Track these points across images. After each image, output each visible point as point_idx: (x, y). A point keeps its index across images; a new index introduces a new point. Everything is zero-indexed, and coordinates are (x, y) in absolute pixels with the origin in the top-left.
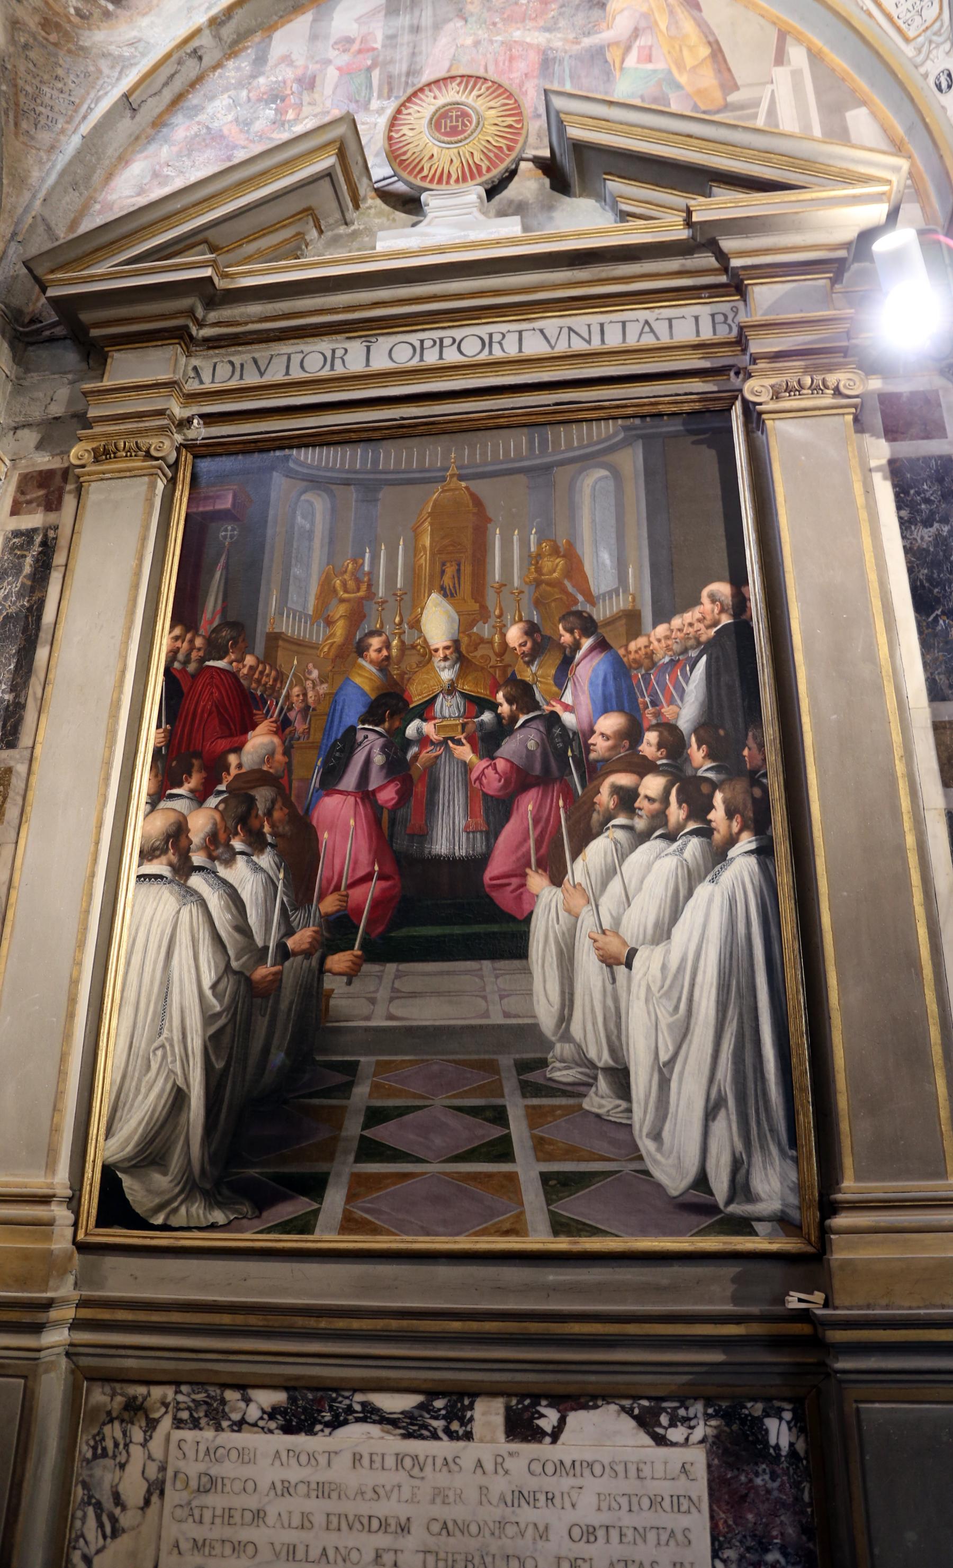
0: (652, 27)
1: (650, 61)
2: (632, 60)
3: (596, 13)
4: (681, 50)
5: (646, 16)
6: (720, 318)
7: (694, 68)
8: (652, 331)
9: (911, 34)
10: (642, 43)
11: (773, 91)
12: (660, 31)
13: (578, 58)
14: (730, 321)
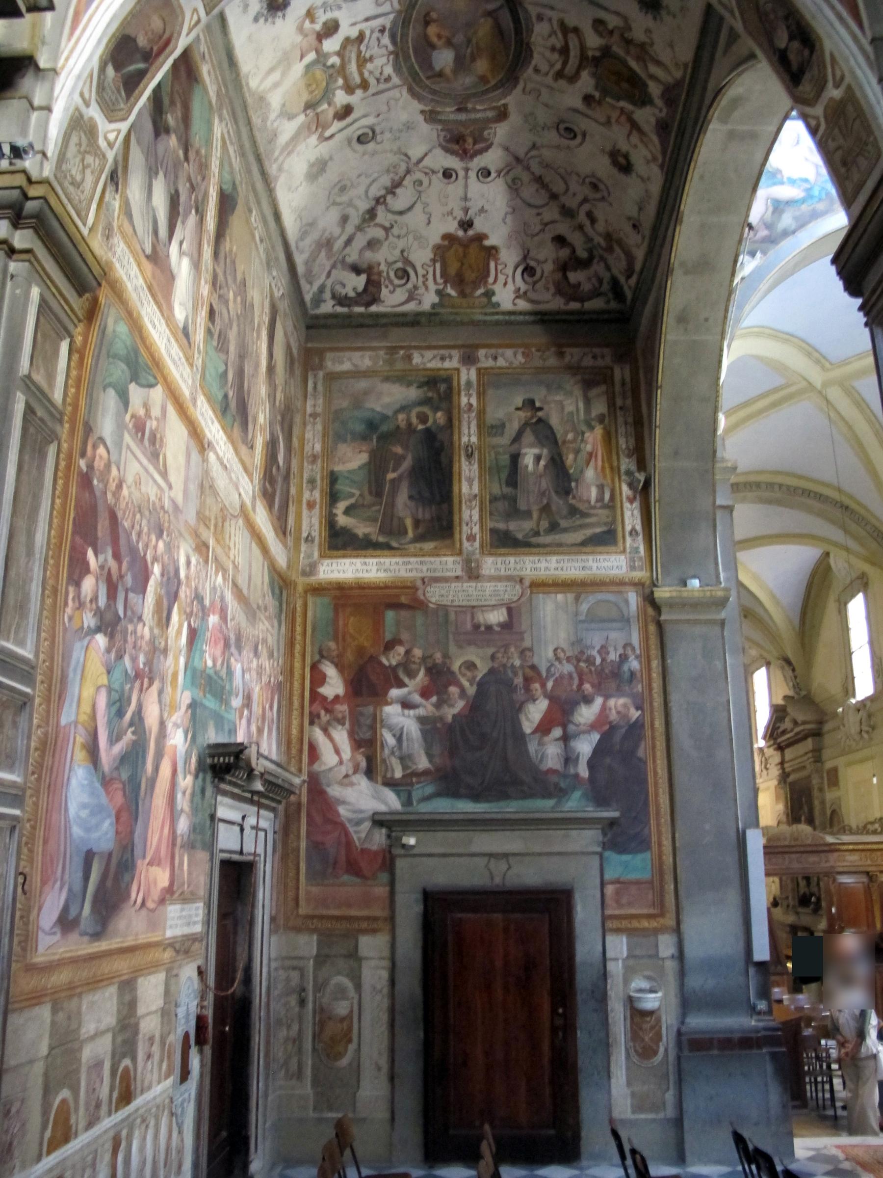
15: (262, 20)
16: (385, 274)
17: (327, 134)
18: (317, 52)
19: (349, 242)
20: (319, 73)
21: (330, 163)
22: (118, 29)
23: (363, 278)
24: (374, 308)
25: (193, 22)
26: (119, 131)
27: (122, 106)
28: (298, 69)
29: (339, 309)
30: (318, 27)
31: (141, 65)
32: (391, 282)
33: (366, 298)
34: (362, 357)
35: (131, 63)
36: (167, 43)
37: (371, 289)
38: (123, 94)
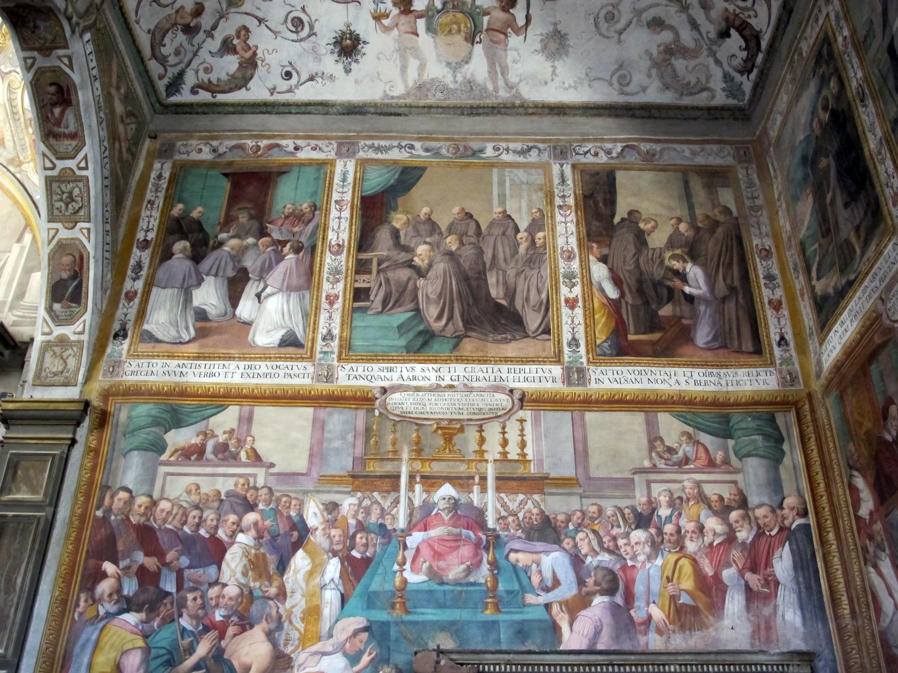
15: (354, 66)
16: (738, 11)
17: (521, 22)
18: (420, 17)
19: (695, 26)
20: (446, 19)
21: (559, 28)
22: (47, 288)
23: (733, 32)
24: (764, 44)
26: (85, 321)
27: (77, 310)
28: (425, 40)
29: (753, 76)
30: (395, 11)
32: (747, 9)
33: (753, 44)
34: (782, 98)
36: (82, 258)
37: (747, 33)
38: (74, 305)
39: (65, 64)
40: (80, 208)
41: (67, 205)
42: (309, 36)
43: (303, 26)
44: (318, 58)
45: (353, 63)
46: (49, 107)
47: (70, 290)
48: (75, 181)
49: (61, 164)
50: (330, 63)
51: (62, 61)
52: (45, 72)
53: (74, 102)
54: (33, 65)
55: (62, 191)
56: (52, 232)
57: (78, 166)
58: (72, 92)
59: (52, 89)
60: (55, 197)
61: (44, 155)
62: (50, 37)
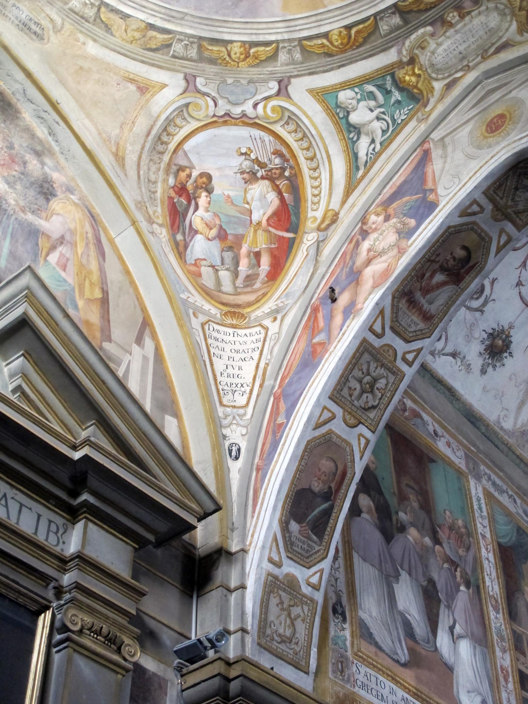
0: (74, 245)
1: (64, 270)
2: (53, 258)
3: (41, 201)
4: (85, 280)
5: (73, 232)
6: (53, 527)
7: (89, 300)
8: (6, 506)
9: (225, 401)
10: (63, 252)
11: (130, 361)
12: (77, 253)
13: (21, 223)
14: (59, 535)
15: (490, 369)
22: (289, 490)
25: (362, 446)
26: (322, 571)
27: (317, 548)
31: (325, 505)
35: (313, 511)
36: (344, 474)
38: (314, 538)
39: (499, 242)
40: (374, 407)
41: (363, 391)
42: (477, 310)
43: (480, 296)
44: (469, 338)
45: (491, 366)
46: (437, 266)
47: (315, 512)
48: (389, 369)
49: (390, 338)
50: (474, 351)
51: (500, 236)
52: (476, 232)
53: (462, 285)
54: (474, 214)
55: (368, 370)
56: (327, 415)
57: (405, 353)
58: (472, 274)
59: (460, 253)
60: (357, 373)
61: (382, 312)
62: (521, 207)
